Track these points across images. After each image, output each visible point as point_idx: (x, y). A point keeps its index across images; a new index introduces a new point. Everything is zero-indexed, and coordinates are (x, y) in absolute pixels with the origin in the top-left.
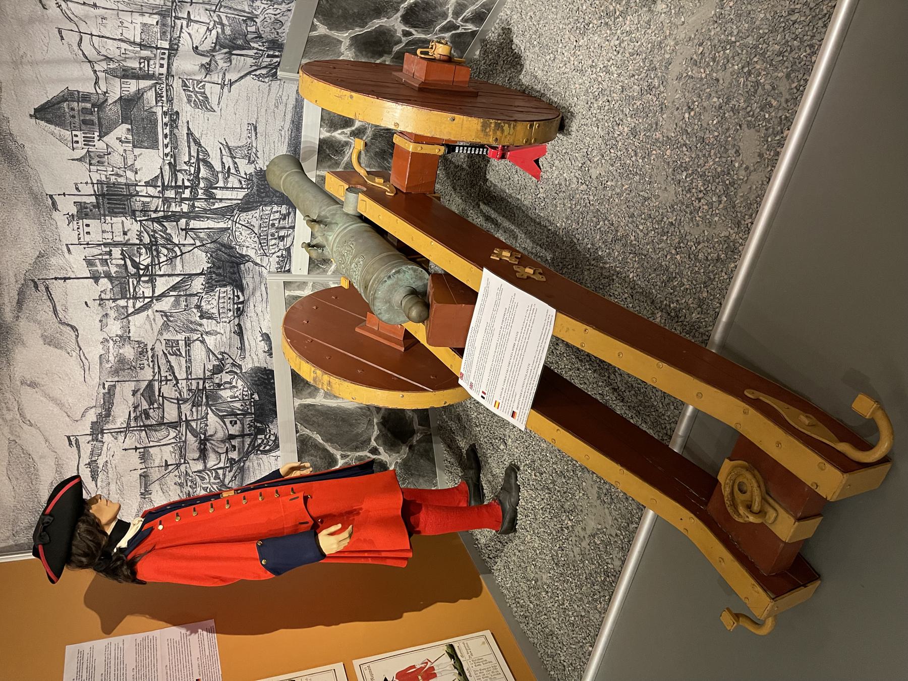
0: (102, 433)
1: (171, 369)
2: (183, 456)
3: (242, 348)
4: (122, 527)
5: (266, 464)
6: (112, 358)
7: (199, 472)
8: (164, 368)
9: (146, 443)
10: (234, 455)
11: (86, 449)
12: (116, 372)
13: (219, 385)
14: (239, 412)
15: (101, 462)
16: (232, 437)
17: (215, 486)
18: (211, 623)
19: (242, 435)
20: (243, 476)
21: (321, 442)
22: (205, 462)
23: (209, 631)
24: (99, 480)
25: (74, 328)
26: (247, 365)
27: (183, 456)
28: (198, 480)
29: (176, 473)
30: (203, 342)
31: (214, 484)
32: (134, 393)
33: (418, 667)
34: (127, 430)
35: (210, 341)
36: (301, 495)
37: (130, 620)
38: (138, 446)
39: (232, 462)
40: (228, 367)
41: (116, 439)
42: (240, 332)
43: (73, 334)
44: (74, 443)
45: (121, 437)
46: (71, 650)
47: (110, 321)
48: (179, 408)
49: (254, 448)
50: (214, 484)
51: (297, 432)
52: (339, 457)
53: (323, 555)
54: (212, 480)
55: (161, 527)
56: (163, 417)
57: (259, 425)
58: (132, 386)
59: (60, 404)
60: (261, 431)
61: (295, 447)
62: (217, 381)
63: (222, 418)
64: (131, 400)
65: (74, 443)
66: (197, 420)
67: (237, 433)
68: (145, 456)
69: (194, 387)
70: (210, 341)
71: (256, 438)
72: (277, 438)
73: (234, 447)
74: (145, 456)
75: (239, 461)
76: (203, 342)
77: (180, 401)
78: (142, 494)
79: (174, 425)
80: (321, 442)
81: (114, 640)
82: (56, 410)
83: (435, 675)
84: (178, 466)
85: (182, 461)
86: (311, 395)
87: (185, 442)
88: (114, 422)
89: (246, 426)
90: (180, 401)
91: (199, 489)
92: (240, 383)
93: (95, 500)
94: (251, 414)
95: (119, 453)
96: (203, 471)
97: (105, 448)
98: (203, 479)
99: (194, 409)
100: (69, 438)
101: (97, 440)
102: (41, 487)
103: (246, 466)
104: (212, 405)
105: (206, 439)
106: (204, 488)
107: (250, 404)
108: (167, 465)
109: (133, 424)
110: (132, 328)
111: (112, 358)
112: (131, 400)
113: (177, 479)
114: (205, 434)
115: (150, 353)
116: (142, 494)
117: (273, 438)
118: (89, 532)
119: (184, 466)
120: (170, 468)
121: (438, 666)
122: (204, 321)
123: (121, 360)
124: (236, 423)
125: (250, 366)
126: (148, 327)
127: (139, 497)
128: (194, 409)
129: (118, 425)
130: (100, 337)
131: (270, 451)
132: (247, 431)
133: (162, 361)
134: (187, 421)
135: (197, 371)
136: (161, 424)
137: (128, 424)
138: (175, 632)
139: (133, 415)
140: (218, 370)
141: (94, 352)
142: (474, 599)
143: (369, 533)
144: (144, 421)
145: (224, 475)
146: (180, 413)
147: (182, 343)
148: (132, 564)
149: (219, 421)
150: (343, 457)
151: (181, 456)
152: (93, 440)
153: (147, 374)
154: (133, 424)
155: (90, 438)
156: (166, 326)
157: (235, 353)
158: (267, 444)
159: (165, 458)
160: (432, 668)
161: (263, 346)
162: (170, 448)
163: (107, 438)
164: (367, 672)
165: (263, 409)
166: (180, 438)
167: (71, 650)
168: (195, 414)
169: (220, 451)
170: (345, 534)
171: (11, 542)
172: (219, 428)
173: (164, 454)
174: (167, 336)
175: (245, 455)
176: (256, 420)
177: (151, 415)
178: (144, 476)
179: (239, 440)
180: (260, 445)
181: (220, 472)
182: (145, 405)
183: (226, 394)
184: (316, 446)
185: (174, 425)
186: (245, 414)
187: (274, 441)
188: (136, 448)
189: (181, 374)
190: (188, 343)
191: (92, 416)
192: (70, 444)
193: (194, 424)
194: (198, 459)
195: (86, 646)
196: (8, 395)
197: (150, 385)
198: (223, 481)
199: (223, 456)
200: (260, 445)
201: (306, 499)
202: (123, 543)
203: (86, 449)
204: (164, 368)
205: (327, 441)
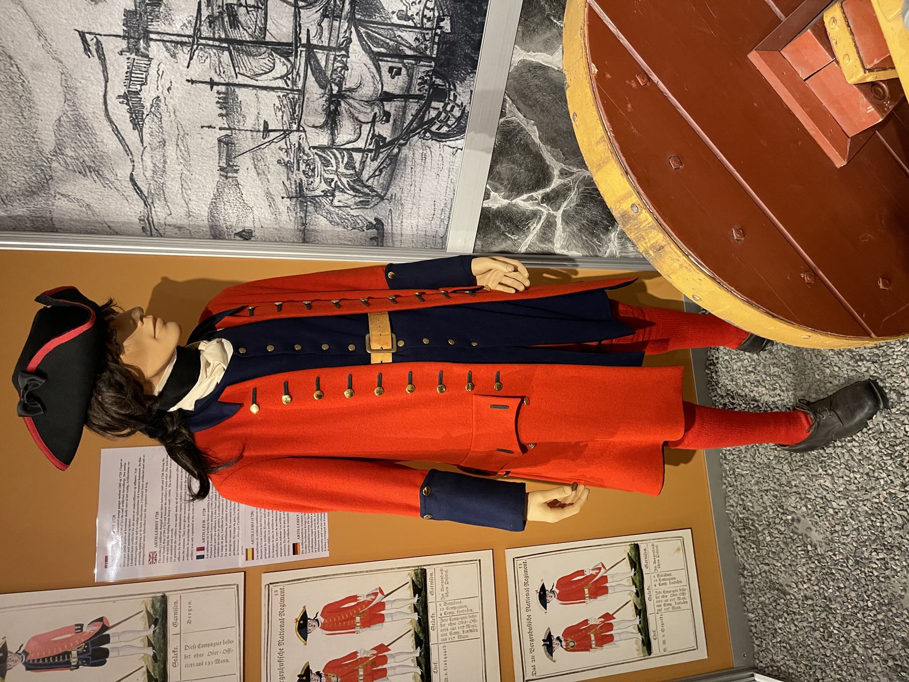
0: (148, 40)
2: (297, 118)
5: (436, 157)
7: (322, 148)
9: (229, 75)
10: (385, 130)
11: (119, 65)
14: (409, 52)
15: (148, 95)
16: (387, 97)
17: (344, 180)
19: (406, 97)
21: (537, 141)
22: (332, 134)
24: (146, 130)
28: (319, 163)
29: (282, 144)
31: (345, 176)
33: (587, 573)
34: (193, 42)
38: (216, 79)
39: (379, 140)
41: (174, 56)
44: (93, 48)
45: (183, 55)
48: (297, 16)
49: (421, 124)
50: (345, 176)
51: (503, 114)
52: (556, 172)
54: (342, 169)
56: (264, 30)
57: (438, 81)
61: (490, 142)
63: (376, 58)
65: (93, 48)
66: (329, 49)
67: (397, 92)
68: (228, 104)
71: (427, 106)
72: (464, 115)
73: (387, 115)
74: (228, 104)
75: (392, 143)
78: (222, 169)
79: (285, 50)
80: (537, 141)
83: (605, 591)
84: (286, 133)
85: (295, 127)
86: (548, 47)
87: (302, 92)
88: (168, 18)
89: (416, 81)
91: (317, 180)
94: (430, 59)
95: (181, 87)
96: (329, 148)
97: (153, 71)
98: (326, 163)
99: (325, 24)
100: (82, 35)
101: (137, 51)
102: (40, 125)
103: (402, 155)
104: (360, 23)
106: (326, 180)
107: (433, 38)
108: (267, 130)
109: (205, 31)
113: (283, 155)
114: (340, 85)
116: (222, 169)
117: (457, 112)
119: (297, 134)
120: (273, 135)
121: (613, 576)
124: (399, 73)
127: (217, 173)
128: (325, 24)
129: (177, 28)
131: (447, 136)
134: (310, 47)
136: (260, 42)
137: (197, 30)
139: (205, 13)
142: (682, 465)
145: (363, 163)
146: (297, 26)
149: (370, 63)
150: (564, 174)
151: (293, 118)
152: (129, 50)
154: (205, 31)
155: (123, 44)
158: (445, 122)
159: (264, 117)
160: (604, 579)
162: (272, 98)
164: (521, 572)
165: (453, 53)
166: (294, 83)
168: (326, 33)
169: (362, 118)
172: (368, 78)
173: (261, 108)
175: (404, 135)
176: (435, 72)
177: (242, 19)
178: (227, 144)
179: (398, 103)
180: (432, 122)
181: (357, 157)
184: (528, 149)
185: (285, 50)
186: (420, 57)
187: (459, 119)
188: (212, 83)
192: (87, 49)
193: (321, 56)
194: (321, 127)
198: (359, 175)
199: (366, 128)
200: (432, 122)
205: (547, 140)
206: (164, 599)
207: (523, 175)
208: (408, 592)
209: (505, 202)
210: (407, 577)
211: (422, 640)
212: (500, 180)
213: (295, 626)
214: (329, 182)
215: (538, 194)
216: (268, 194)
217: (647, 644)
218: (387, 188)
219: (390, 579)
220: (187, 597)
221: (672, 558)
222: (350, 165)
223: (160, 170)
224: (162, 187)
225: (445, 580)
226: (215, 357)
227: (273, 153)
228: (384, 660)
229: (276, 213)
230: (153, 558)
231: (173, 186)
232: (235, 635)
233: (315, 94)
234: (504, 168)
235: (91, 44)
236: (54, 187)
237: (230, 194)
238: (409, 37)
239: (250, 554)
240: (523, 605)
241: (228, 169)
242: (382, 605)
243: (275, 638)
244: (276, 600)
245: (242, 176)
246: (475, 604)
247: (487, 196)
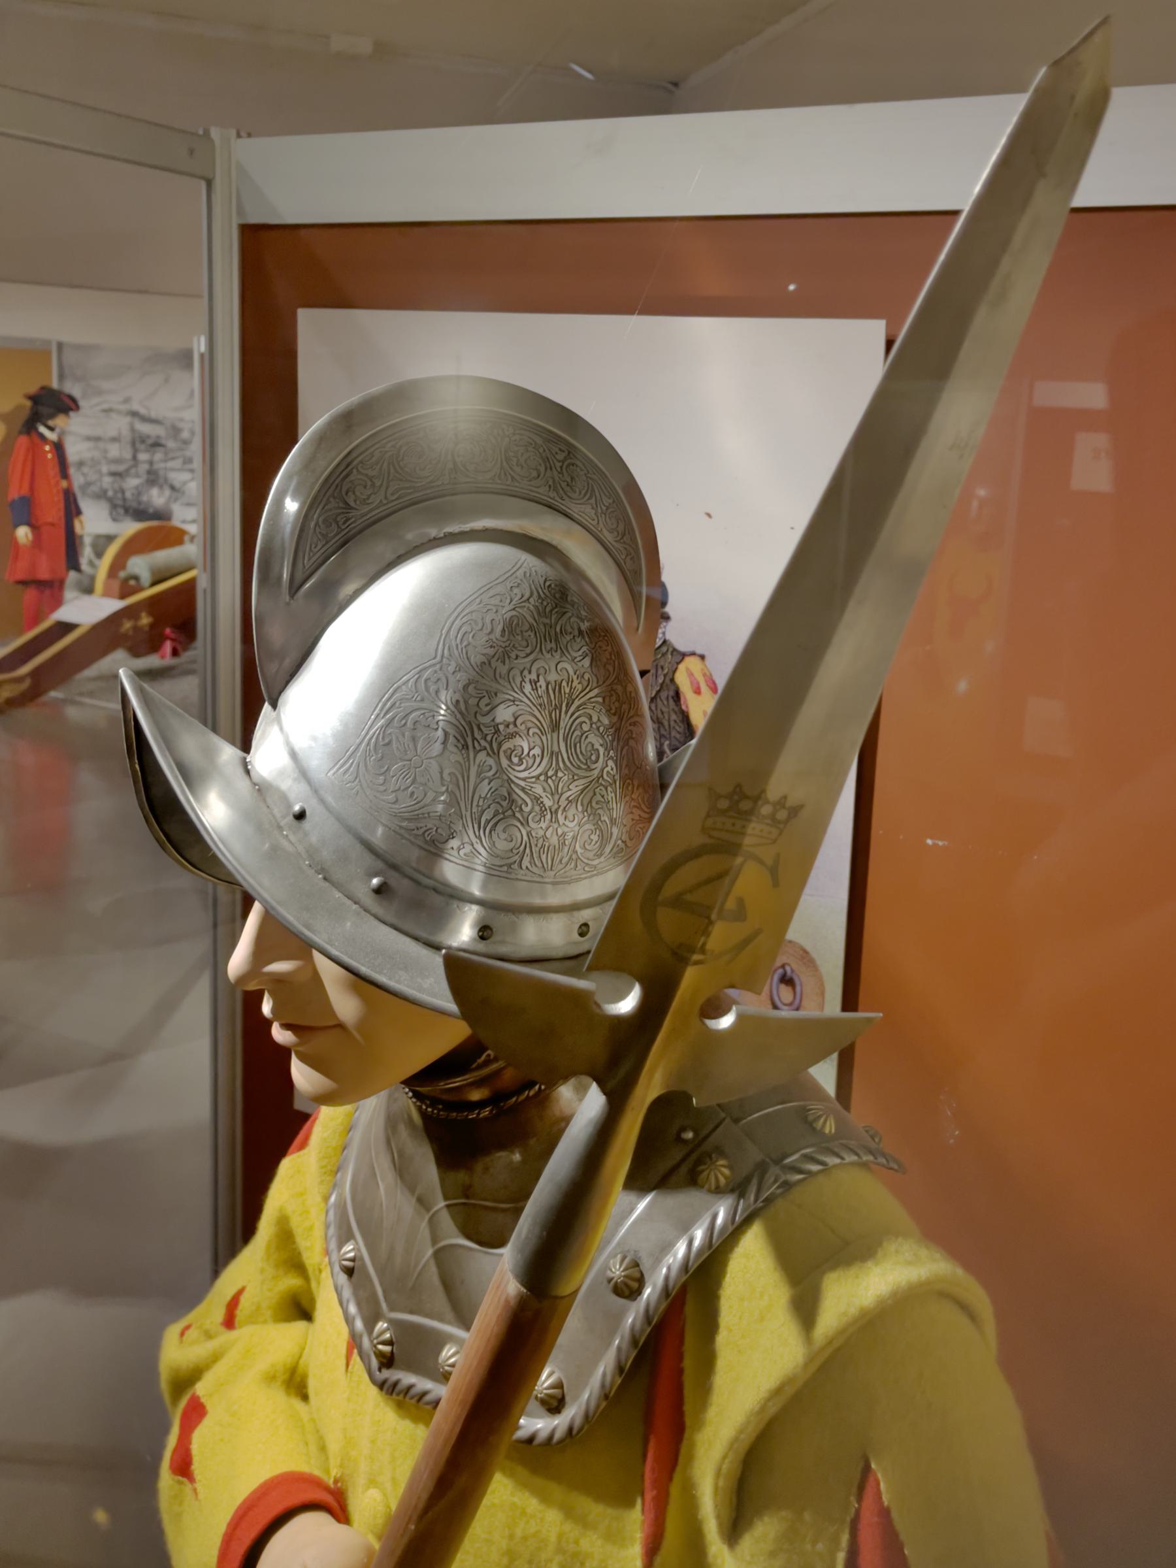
1: (173, 459)
4: (51, 429)
11: (123, 407)
34: (133, 430)
68: (115, 440)
74: (115, 440)
77: (151, 463)
79: (134, 458)
140: (173, 488)
144: (138, 442)
153: (171, 444)
163: (128, 419)
173: (114, 451)
175: (110, 500)
185: (134, 458)
189: (170, 464)
190: (192, 471)
191: (143, 411)
233: (121, 468)
235: (127, 400)
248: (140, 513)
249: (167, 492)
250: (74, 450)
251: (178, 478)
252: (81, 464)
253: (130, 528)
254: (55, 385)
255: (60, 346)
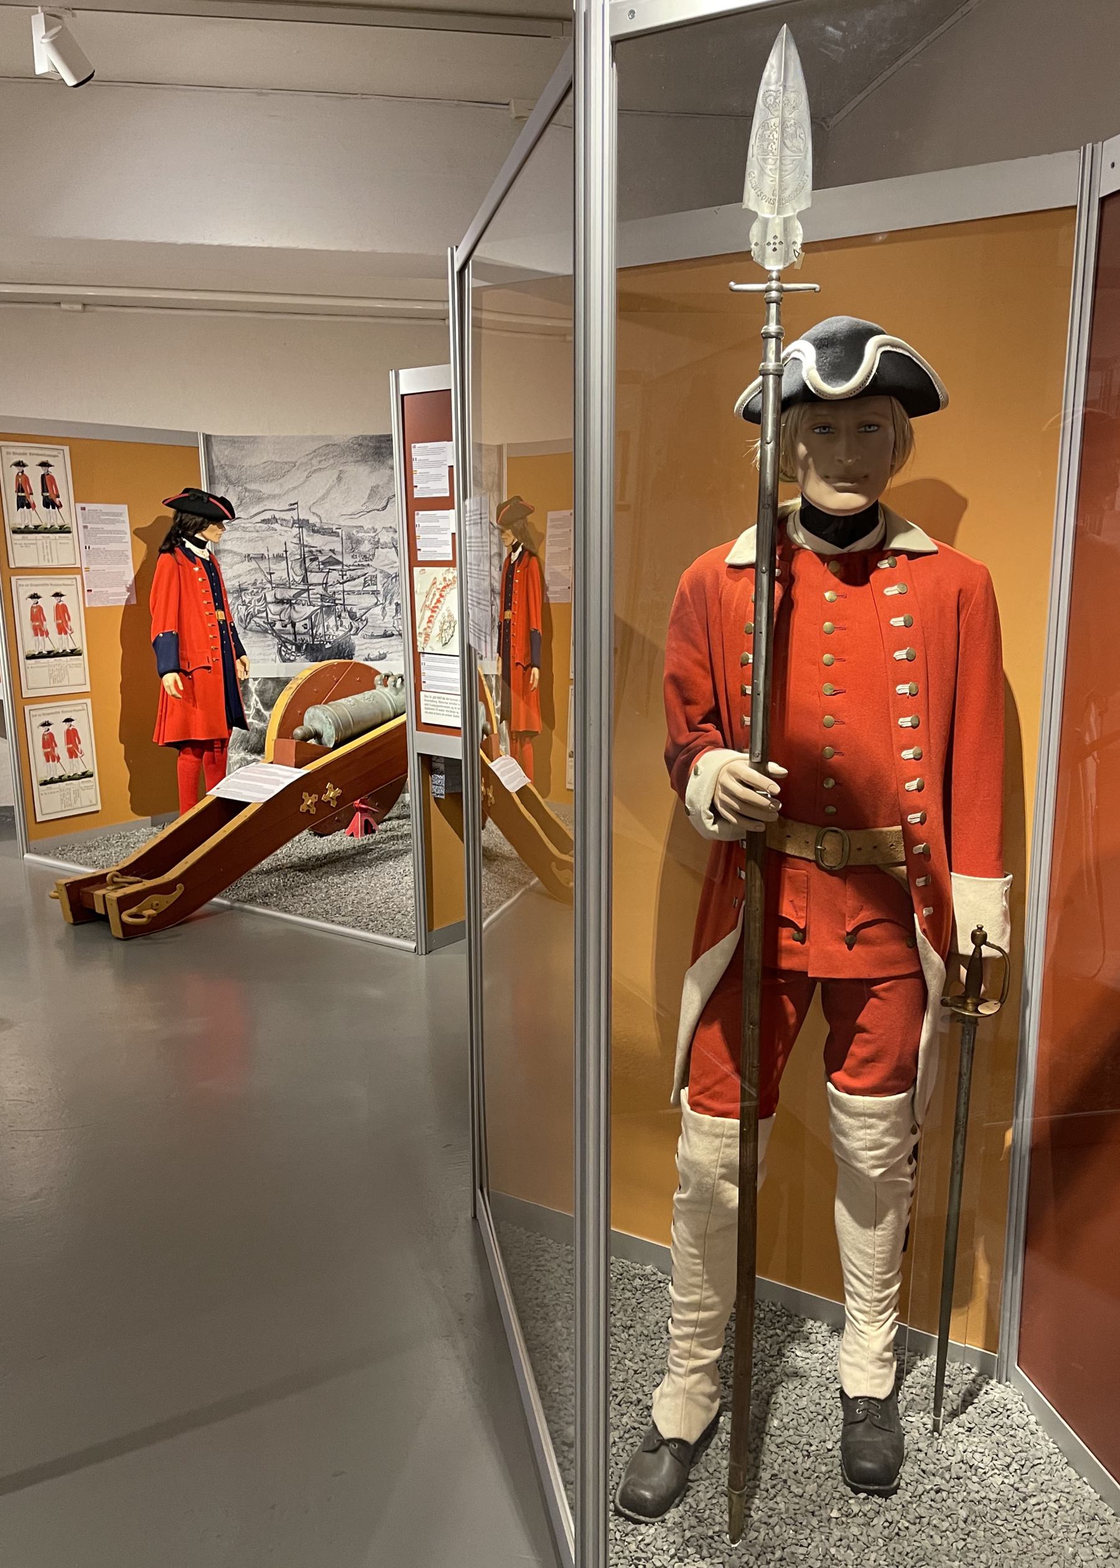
2: (278, 586)
3: (372, 636)
4: (201, 545)
6: (360, 535)
8: (353, 573)
10: (278, 626)
11: (287, 516)
12: (350, 538)
13: (340, 616)
15: (275, 526)
16: (294, 625)
18: (134, 602)
19: (295, 634)
20: (257, 632)
23: (128, 600)
25: (384, 508)
26: (356, 640)
27: (278, 586)
30: (376, 605)
32: (333, 551)
35: (378, 610)
36: (210, 665)
37: (143, 547)
40: (355, 624)
42: (386, 635)
43: (380, 507)
45: (296, 540)
46: (124, 508)
47: (391, 534)
53: (162, 676)
55: (197, 569)
58: (338, 548)
59: (323, 498)
60: (298, 649)
62: (343, 615)
63: (310, 617)
64: (327, 548)
68: (278, 558)
69: (337, 596)
70: (378, 610)
71: (292, 644)
74: (278, 558)
76: (376, 605)
79: (305, 580)
81: (128, 537)
82: (320, 495)
83: (71, 757)
84: (271, 582)
88: (308, 536)
90: (325, 585)
92: (341, 633)
93: (222, 527)
95: (283, 539)
98: (259, 601)
101: (294, 523)
105: (291, 604)
108: (271, 574)
109: (306, 549)
110: (385, 550)
111: (360, 535)
112: (327, 548)
115: (365, 563)
117: (292, 658)
118: (195, 524)
122: (394, 606)
123: (359, 542)
125: (356, 642)
126: (386, 562)
130: (378, 527)
132: (298, 637)
133: (359, 572)
134: (308, 590)
135: (350, 599)
138: (130, 577)
140: (352, 616)
141: (366, 522)
143: (178, 711)
144: (308, 557)
146: (316, 585)
147: (375, 588)
148: (171, 550)
153: (348, 561)
156: (388, 576)
157: (368, 631)
160: (76, 756)
161: (375, 654)
163: (296, 530)
164: (80, 707)
167: (124, 508)
170: (175, 692)
171: (215, 464)
173: (280, 572)
174: (380, 576)
178: (262, 557)
179: (291, 630)
181: (264, 614)
182: (321, 559)
183: (332, 621)
185: (305, 580)
186: (313, 636)
189: (347, 586)
191: (313, 520)
193: (306, 595)
195: (126, 518)
196: (331, 461)
197: (338, 563)
201: (208, 668)
202: (188, 545)
203: (287, 516)
204: (353, 573)
206: (69, 532)
207: (268, 696)
208: (72, 647)
209: (253, 690)
210: (78, 646)
211: (51, 655)
212: (264, 685)
213: (58, 591)
214: (250, 602)
215: (260, 706)
216: (240, 576)
217: (45, 783)
218: (251, 630)
219: (77, 639)
220: (70, 542)
221: (86, 797)
222: (259, 611)
223: (245, 529)
224: (236, 529)
225: (77, 666)
226: (202, 554)
227: (259, 577)
228: (42, 635)
229: (230, 579)
230: (85, 527)
231: (238, 534)
232: (55, 564)
233: (289, 594)
234: (270, 684)
235: (293, 507)
236: (231, 487)
237: (237, 559)
238: (321, 631)
239: (87, 569)
240: (65, 709)
241: (249, 557)
242: (66, 633)
243: (54, 582)
244: (69, 582)
245: (246, 563)
246: (65, 682)
247: (255, 679)
248: (314, 651)
249: (347, 622)
250: (232, 574)
251: (359, 603)
252: (241, 590)
253: (303, 669)
254: (204, 489)
255: (208, 438)
